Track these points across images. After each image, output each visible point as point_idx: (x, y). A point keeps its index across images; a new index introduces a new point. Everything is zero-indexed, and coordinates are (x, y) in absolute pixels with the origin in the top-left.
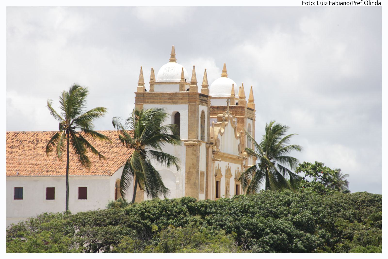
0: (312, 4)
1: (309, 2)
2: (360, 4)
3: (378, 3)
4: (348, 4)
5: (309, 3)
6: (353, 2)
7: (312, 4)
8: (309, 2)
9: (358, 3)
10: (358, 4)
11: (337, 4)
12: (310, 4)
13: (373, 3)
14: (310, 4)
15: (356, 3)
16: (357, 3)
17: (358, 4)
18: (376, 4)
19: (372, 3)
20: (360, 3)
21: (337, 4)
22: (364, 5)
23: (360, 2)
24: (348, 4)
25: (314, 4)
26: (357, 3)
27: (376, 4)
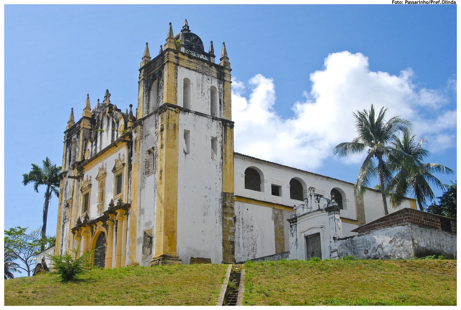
1: (398, 1)
2: (438, 3)
3: (454, 2)
6: (432, 2)
8: (398, 1)
9: (436, 3)
13: (449, 2)
16: (435, 3)
19: (448, 2)
22: (442, 4)
23: (438, 1)
25: (402, 3)
26: (435, 3)
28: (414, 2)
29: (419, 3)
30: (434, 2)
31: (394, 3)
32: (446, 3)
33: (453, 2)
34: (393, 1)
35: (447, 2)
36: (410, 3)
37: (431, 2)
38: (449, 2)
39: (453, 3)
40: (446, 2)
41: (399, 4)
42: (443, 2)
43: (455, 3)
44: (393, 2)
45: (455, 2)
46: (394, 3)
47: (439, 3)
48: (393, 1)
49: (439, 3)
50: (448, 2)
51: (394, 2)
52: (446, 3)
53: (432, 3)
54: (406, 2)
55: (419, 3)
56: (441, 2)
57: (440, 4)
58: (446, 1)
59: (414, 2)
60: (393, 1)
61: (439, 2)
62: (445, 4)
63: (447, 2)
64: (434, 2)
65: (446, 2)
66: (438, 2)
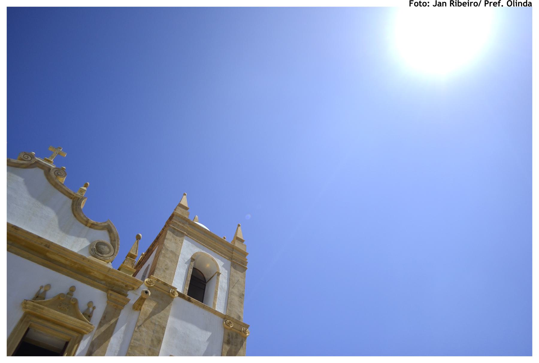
0: (425, 4)
1: (420, 2)
2: (498, 5)
5: (419, 3)
6: (487, 2)
7: (425, 4)
8: (420, 2)
9: (494, 4)
10: (495, 5)
11: (460, 4)
12: (421, 4)
13: (520, 4)
14: (421, 4)
15: (490, 3)
16: (492, 4)
17: (495, 5)
18: (525, 4)
19: (519, 3)
20: (498, 3)
21: (460, 4)
25: (427, 4)
26: (492, 4)
27: (525, 4)
30: (490, 3)
32: (514, 6)
33: (526, 2)
34: (411, 2)
35: (516, 3)
37: (485, 4)
38: (520, 4)
39: (526, 6)
40: (515, 4)
41: (422, 6)
42: (510, 3)
43: (531, 6)
44: (410, 3)
45: (531, 4)
47: (499, 6)
48: (410, 1)
49: (499, 6)
50: (519, 3)
52: (514, 6)
58: (515, 1)
60: (411, 2)
61: (499, 2)
63: (516, 3)
64: (490, 3)
65: (515, 4)
66: (497, 4)
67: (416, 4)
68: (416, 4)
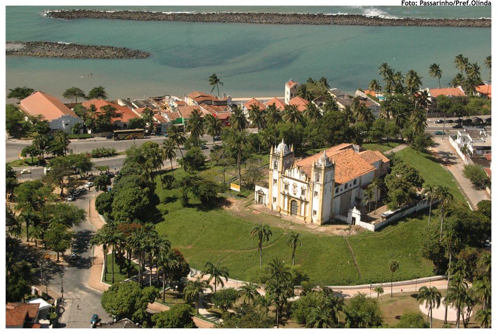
0: (413, 4)
1: (410, 2)
2: (466, 4)
4: (451, 4)
7: (413, 4)
8: (410, 2)
9: (463, 4)
12: (411, 4)
14: (411, 4)
16: (462, 4)
18: (486, 4)
22: (471, 5)
24: (451, 4)
25: (416, 4)
26: (462, 4)
27: (486, 4)
28: (433, 3)
29: (439, 4)
31: (404, 4)
33: (487, 2)
36: (427, 4)
37: (457, 3)
42: (474, 3)
44: (402, 3)
45: (490, 3)
46: (404, 4)
51: (405, 2)
53: (458, 5)
54: (421, 3)
55: (439, 4)
56: (470, 3)
57: (468, 5)
59: (433, 3)
61: (467, 2)
62: (476, 5)
67: (407, 4)
68: (407, 4)
